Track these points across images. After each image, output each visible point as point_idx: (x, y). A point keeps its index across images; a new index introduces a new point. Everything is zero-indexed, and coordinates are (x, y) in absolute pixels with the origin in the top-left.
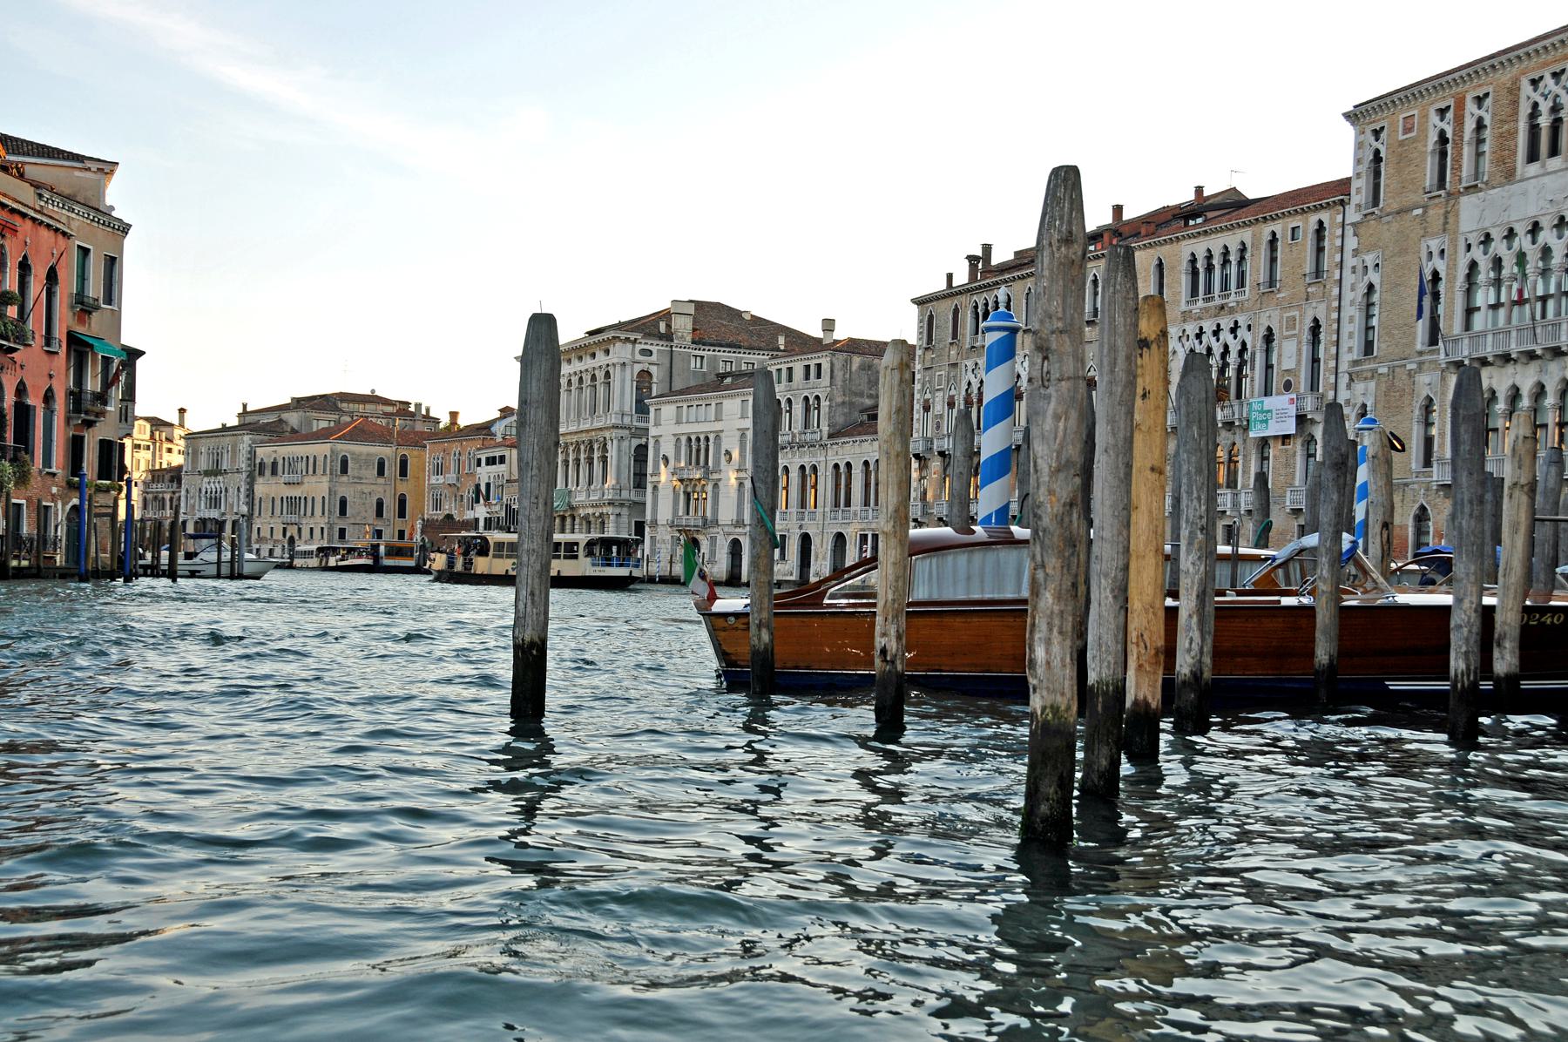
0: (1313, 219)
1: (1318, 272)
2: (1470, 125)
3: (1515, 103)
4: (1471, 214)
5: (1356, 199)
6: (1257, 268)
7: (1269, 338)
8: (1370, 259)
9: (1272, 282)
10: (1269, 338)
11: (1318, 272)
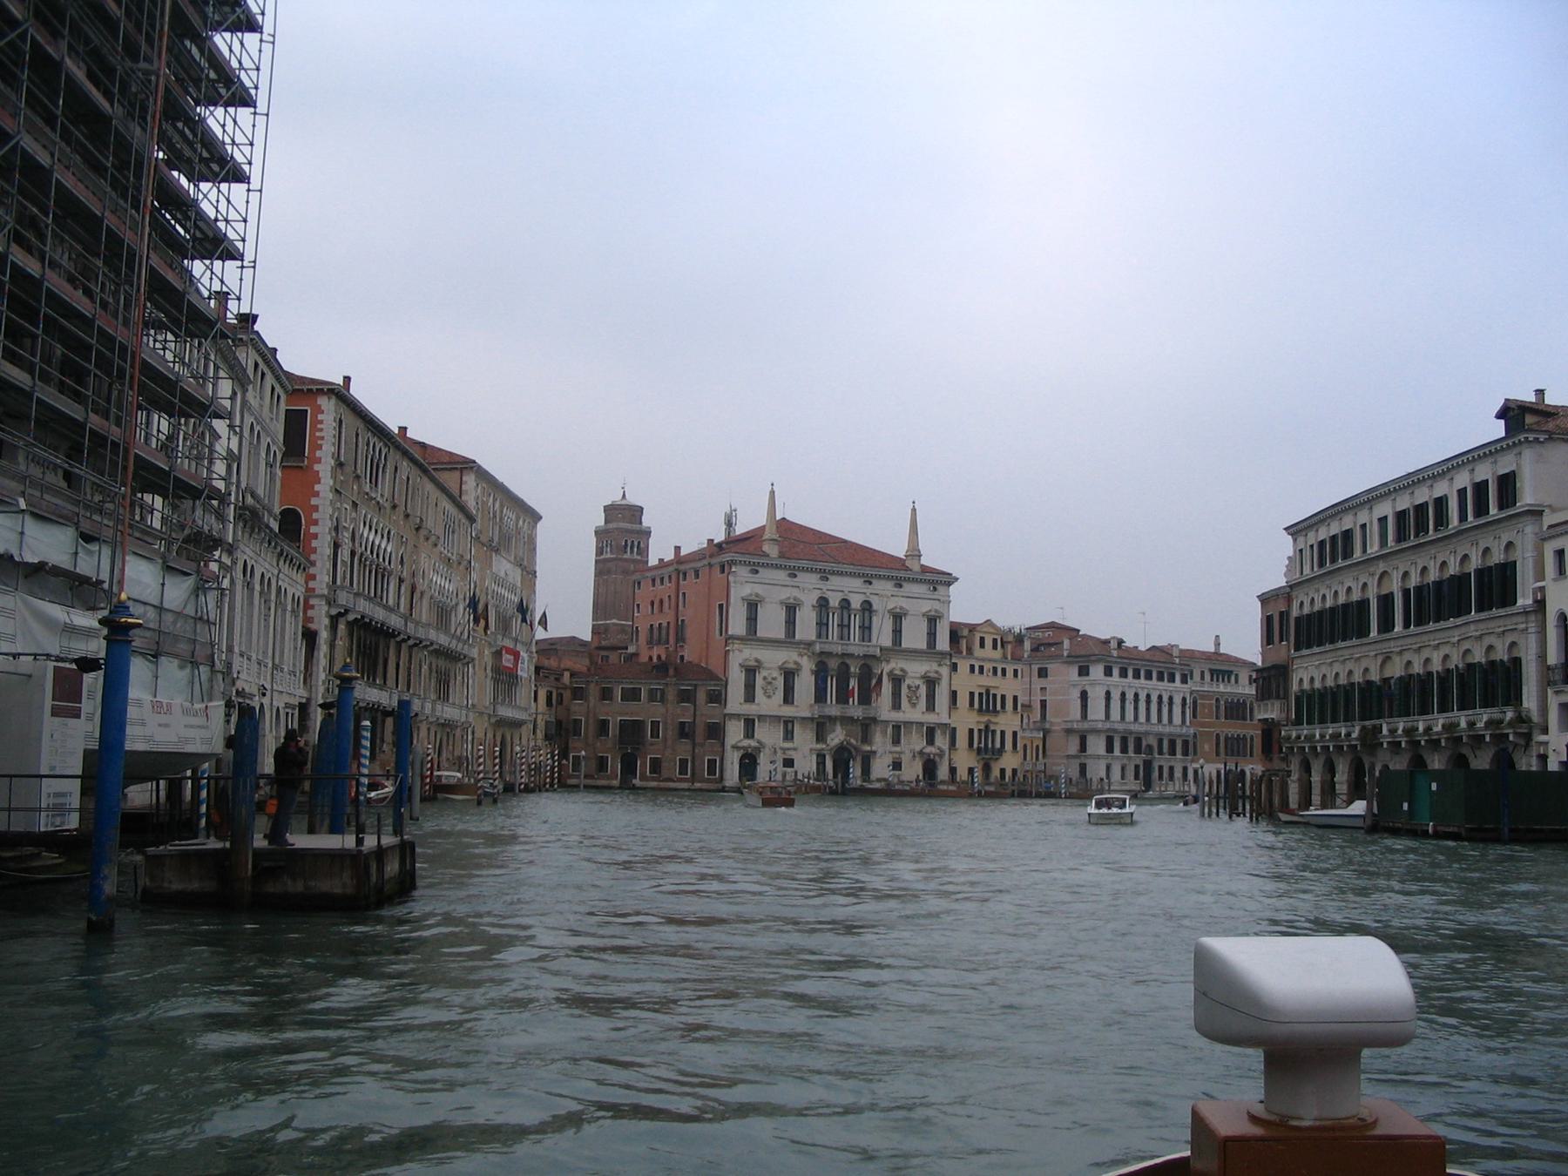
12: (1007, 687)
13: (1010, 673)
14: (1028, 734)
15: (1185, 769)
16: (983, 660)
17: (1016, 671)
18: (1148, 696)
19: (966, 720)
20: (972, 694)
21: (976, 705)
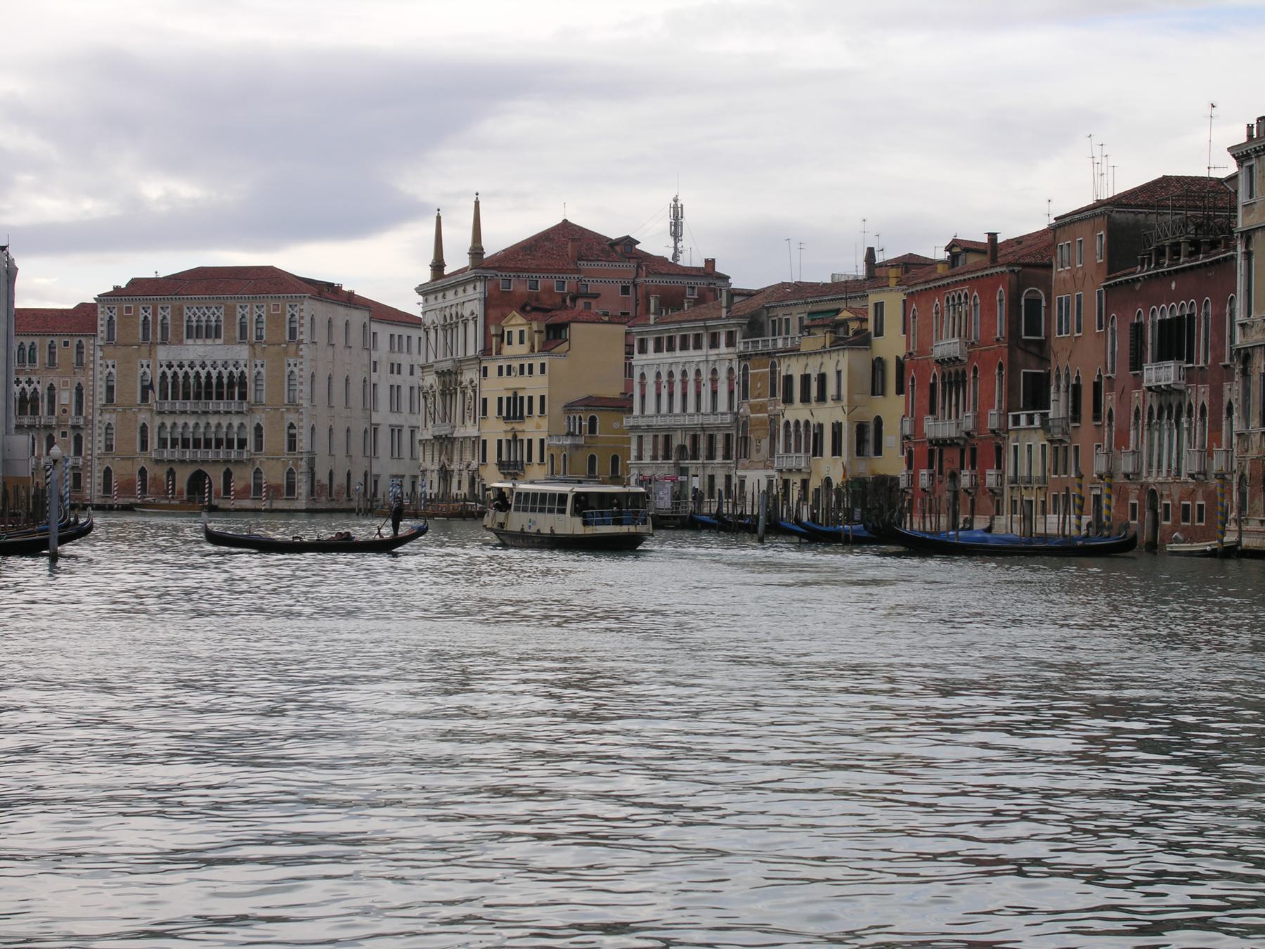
0: (76, 340)
1: (80, 363)
2: (160, 318)
3: (181, 315)
4: (163, 354)
5: (100, 335)
6: (42, 356)
7: (51, 388)
8: (110, 363)
9: (52, 364)
10: (51, 388)
12: (534, 386)
13: (537, 369)
14: (555, 441)
15: (728, 478)
16: (510, 358)
17: (543, 365)
18: (684, 373)
19: (495, 430)
20: (500, 400)
21: (504, 414)
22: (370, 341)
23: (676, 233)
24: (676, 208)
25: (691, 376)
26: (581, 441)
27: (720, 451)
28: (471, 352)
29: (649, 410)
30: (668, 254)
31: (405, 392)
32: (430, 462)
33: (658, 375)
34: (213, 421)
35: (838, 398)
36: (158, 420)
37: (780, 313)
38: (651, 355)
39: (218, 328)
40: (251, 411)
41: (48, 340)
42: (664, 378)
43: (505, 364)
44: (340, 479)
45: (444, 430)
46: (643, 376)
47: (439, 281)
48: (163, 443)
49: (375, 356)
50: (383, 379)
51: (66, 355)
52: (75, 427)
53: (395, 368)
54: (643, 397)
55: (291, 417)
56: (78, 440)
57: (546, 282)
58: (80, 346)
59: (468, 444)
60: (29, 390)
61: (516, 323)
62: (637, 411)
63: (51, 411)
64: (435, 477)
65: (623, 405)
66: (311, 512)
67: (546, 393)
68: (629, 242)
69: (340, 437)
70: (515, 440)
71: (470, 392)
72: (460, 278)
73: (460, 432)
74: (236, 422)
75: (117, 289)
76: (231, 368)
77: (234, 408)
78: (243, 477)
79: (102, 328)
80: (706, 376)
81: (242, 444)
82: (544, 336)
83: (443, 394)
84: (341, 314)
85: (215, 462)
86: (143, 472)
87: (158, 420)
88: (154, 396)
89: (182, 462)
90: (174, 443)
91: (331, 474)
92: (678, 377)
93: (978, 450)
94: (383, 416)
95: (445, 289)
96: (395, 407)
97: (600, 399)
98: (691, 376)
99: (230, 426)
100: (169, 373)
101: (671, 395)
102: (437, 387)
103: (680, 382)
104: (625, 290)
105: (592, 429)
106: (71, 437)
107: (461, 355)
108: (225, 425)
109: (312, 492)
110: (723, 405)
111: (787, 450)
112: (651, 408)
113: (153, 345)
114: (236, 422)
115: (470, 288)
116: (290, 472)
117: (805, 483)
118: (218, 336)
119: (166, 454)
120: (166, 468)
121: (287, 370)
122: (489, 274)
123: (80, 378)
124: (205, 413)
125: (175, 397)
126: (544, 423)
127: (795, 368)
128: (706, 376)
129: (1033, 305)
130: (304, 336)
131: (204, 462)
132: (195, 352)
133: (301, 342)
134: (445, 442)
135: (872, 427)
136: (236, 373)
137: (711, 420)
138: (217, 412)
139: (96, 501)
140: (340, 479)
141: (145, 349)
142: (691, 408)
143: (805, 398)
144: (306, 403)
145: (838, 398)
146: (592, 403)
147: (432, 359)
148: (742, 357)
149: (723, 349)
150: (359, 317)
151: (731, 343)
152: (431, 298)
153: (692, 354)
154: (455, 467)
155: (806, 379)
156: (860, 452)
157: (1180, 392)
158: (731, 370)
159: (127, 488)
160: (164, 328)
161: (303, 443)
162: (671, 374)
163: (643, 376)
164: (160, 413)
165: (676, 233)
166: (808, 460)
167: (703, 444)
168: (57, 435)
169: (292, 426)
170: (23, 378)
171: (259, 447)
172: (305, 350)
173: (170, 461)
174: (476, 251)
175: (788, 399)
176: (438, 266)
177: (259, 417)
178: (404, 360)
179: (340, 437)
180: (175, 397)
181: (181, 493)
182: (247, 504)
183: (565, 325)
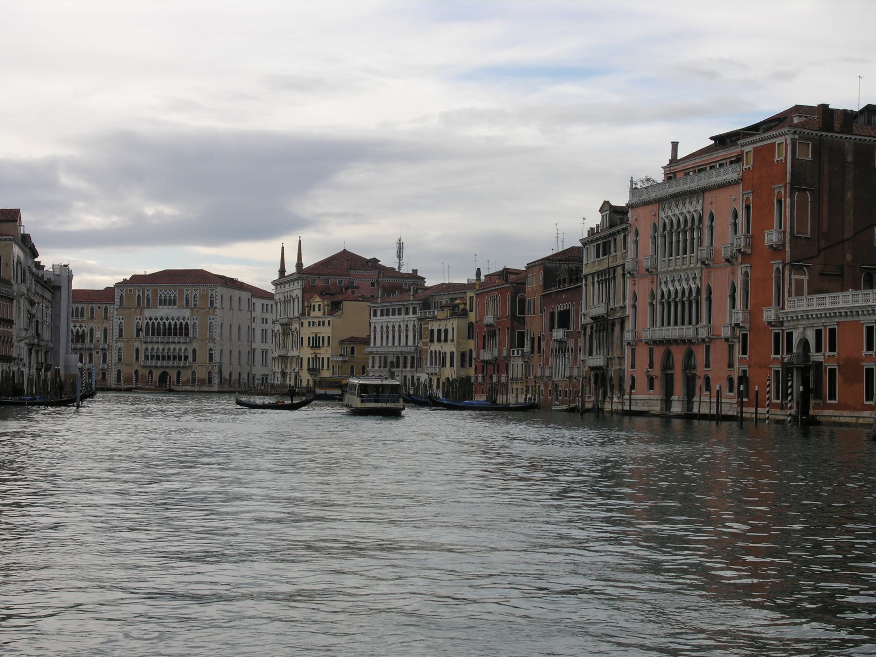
1: (106, 317)
4: (147, 313)
6: (87, 314)
7: (92, 330)
9: (92, 317)
10: (92, 330)
11: (106, 317)
12: (325, 332)
13: (326, 323)
15: (413, 377)
16: (314, 318)
18: (393, 327)
19: (306, 353)
22: (251, 308)
23: (400, 256)
24: (400, 243)
25: (397, 328)
26: (347, 359)
27: (409, 365)
28: (296, 315)
29: (378, 344)
30: (396, 267)
31: (269, 332)
32: (277, 369)
33: (382, 327)
34: (172, 346)
35: (453, 340)
36: (144, 346)
37: (438, 299)
38: (379, 317)
39: (175, 300)
40: (191, 342)
41: (90, 306)
42: (385, 329)
43: (312, 321)
44: (235, 376)
45: (283, 353)
46: (375, 327)
47: (283, 278)
48: (147, 358)
49: (254, 315)
50: (258, 327)
51: (99, 313)
52: (103, 349)
53: (264, 321)
54: (375, 338)
55: (210, 345)
56: (105, 356)
57: (332, 280)
58: (106, 309)
59: (294, 359)
60: (80, 330)
61: (317, 301)
62: (372, 344)
63: (91, 341)
64: (279, 375)
65: (366, 342)
66: (220, 392)
67: (330, 335)
68: (375, 261)
69: (235, 355)
70: (316, 358)
71: (295, 334)
72: (291, 278)
73: (291, 354)
74: (183, 347)
75: (125, 280)
76: (181, 320)
77: (182, 340)
78: (186, 375)
79: (117, 300)
80: (403, 328)
81: (186, 358)
82: (330, 308)
83: (283, 334)
84: (236, 294)
85: (173, 367)
86: (136, 372)
87: (144, 346)
88: (142, 334)
89: (156, 367)
90: (152, 357)
91: (231, 374)
92: (391, 328)
93: (499, 365)
94: (258, 345)
95: (285, 283)
96: (264, 339)
97: (357, 338)
98: (397, 328)
99: (180, 349)
100: (150, 323)
101: (387, 337)
102: (281, 331)
103: (390, 330)
104: (373, 284)
105: (352, 353)
106: (101, 354)
107: (291, 316)
108: (177, 349)
109: (221, 382)
110: (410, 343)
111: (431, 364)
112: (378, 343)
113: (142, 308)
114: (183, 347)
115: (296, 283)
116: (210, 373)
117: (438, 380)
118: (175, 304)
119: (148, 363)
120: (148, 370)
121: (209, 322)
122: (305, 276)
123: (106, 325)
124: (168, 343)
125: (153, 334)
126: (330, 349)
127: (435, 326)
128: (403, 328)
129: (522, 301)
130: (217, 305)
131: (167, 367)
132: (163, 312)
133: (216, 308)
134: (284, 359)
135: (468, 354)
136: (184, 323)
137: (405, 349)
138: (174, 342)
139: (113, 386)
140: (235, 376)
141: (138, 311)
142: (396, 344)
143: (439, 340)
144: (218, 338)
145: (453, 340)
146: (353, 340)
147: (278, 317)
148: (420, 319)
149: (411, 315)
150: (245, 295)
151: (414, 313)
152: (279, 287)
153: (397, 318)
154: (288, 371)
155: (439, 331)
156: (462, 365)
157: (566, 342)
158: (414, 325)
159: (129, 380)
160: (148, 300)
161: (217, 358)
162: (387, 327)
163: (375, 327)
164: (145, 342)
165: (400, 256)
166: (440, 369)
167: (401, 361)
168: (94, 353)
169: (211, 349)
170: (78, 325)
171: (194, 360)
172: (218, 312)
173: (150, 367)
174: (299, 265)
175: (432, 341)
176: (282, 271)
177: (195, 345)
178: (270, 317)
179: (235, 355)
180: (153, 334)
181: (155, 383)
182: (188, 388)
183: (340, 302)
